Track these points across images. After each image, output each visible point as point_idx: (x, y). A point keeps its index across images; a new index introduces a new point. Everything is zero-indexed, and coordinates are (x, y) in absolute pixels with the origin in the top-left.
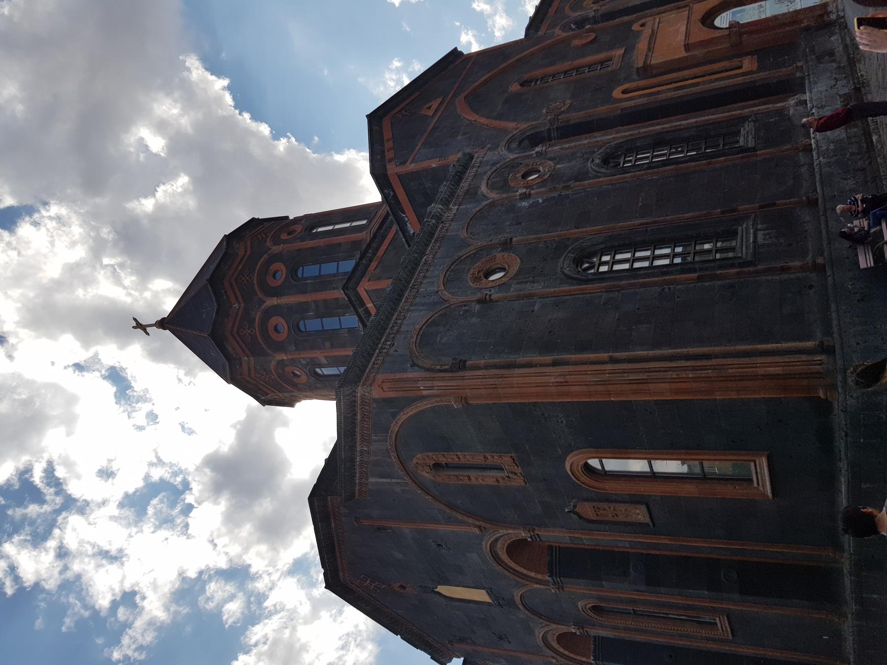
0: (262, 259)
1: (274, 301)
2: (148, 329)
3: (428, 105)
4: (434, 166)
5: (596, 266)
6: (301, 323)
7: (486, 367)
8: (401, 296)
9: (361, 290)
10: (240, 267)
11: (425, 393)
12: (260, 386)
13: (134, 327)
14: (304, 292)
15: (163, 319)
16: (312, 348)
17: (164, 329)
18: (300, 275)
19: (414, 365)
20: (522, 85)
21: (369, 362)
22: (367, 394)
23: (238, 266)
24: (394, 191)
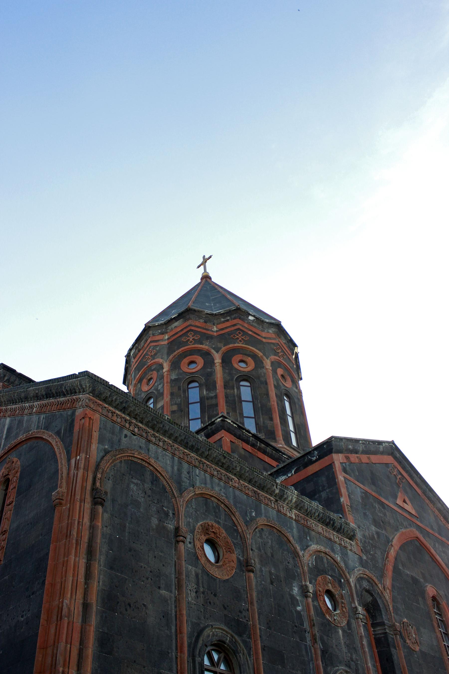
0: (257, 351)
1: (218, 360)
2: (202, 267)
3: (407, 500)
4: (342, 500)
5: (213, 668)
6: (196, 384)
7: (92, 527)
8: (192, 448)
9: (222, 434)
10: (250, 333)
11: (73, 461)
12: (141, 351)
13: (204, 256)
14: (226, 386)
15: (210, 278)
16: (172, 394)
17: (202, 279)
18: (242, 383)
19: (107, 452)
20: (434, 598)
21: (116, 407)
22: (80, 403)
23: (251, 331)
24: (317, 460)
